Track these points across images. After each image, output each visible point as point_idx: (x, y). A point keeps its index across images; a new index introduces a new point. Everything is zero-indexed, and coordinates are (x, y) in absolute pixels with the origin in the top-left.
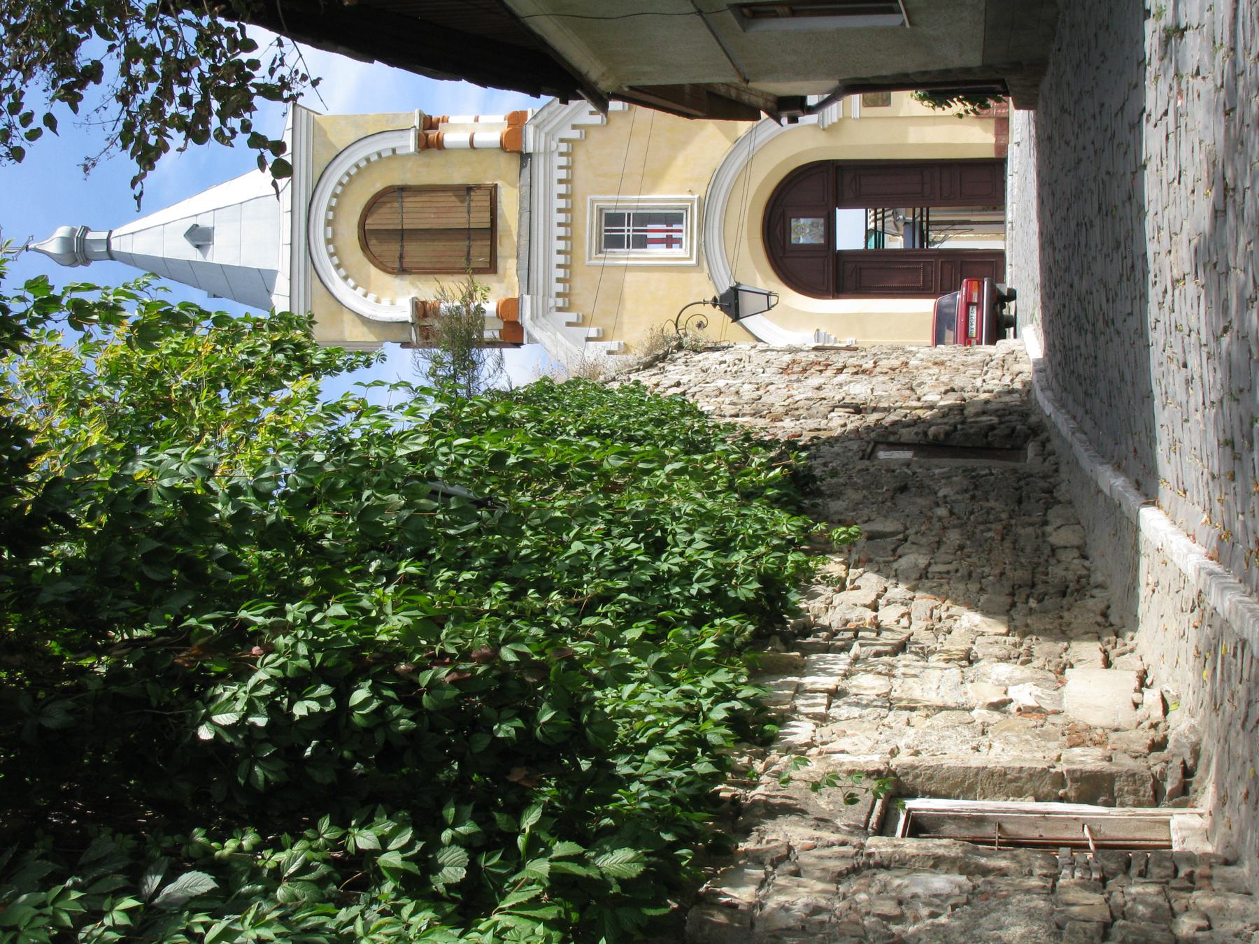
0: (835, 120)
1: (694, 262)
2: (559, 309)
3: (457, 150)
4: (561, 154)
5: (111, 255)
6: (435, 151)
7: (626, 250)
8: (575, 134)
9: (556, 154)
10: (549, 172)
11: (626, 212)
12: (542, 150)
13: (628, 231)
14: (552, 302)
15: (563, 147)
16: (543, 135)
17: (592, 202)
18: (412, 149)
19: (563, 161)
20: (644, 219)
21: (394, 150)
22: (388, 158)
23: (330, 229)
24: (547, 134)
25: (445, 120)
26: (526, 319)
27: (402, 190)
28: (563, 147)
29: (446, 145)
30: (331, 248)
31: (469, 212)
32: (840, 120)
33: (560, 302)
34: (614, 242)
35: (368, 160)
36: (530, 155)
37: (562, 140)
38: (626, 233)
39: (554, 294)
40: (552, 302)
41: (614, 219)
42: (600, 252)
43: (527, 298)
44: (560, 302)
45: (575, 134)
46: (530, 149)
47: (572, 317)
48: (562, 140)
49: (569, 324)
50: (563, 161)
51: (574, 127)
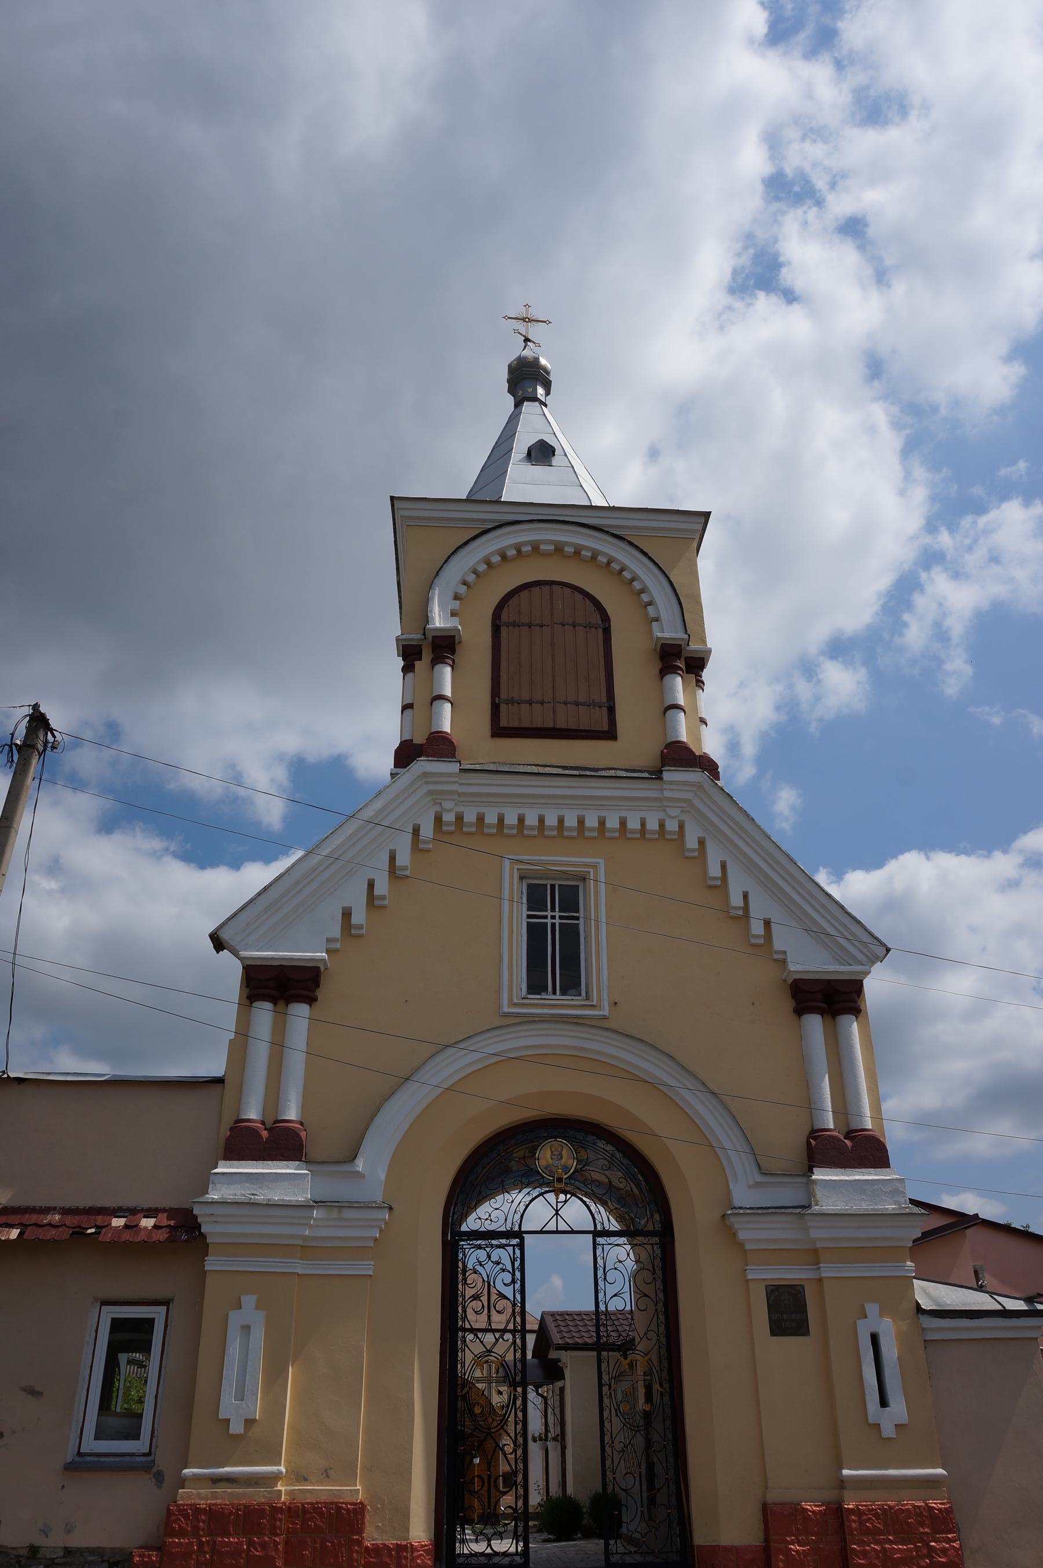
0: (742, 1235)
1: (506, 1009)
2: (438, 820)
3: (662, 692)
4: (662, 825)
5: (518, 404)
6: (657, 666)
7: (525, 913)
8: (691, 843)
9: (662, 815)
10: (636, 807)
11: (581, 914)
12: (667, 794)
13: (553, 917)
14: (447, 805)
15: (672, 826)
16: (689, 796)
17: (595, 866)
18: (659, 635)
19: (652, 825)
20: (571, 937)
21: (657, 620)
22: (647, 614)
23: (552, 547)
24: (688, 801)
25: (700, 684)
26: (422, 765)
27: (607, 632)
28: (672, 826)
29: (668, 678)
30: (526, 549)
31: (577, 704)
32: (741, 1245)
33: (449, 817)
34: (536, 898)
35: (642, 591)
36: (660, 778)
37: (681, 826)
38: (549, 914)
39: (460, 809)
40: (447, 805)
41: (570, 899)
42: (521, 878)
43: (454, 768)
44: (449, 817)
45: (691, 843)
46: (666, 776)
47: (427, 831)
48: (681, 826)
49: (416, 831)
50: (652, 825)
51: (702, 842)
